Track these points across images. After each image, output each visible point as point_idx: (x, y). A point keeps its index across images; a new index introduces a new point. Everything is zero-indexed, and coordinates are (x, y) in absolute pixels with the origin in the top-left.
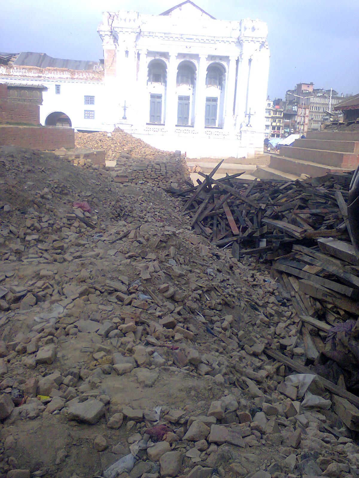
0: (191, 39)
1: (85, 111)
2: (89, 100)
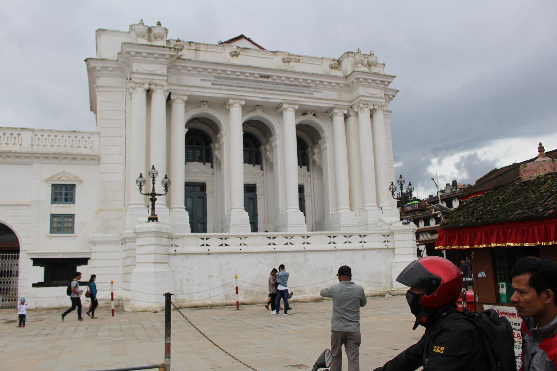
0: (268, 77)
1: (53, 216)
2: (64, 192)
